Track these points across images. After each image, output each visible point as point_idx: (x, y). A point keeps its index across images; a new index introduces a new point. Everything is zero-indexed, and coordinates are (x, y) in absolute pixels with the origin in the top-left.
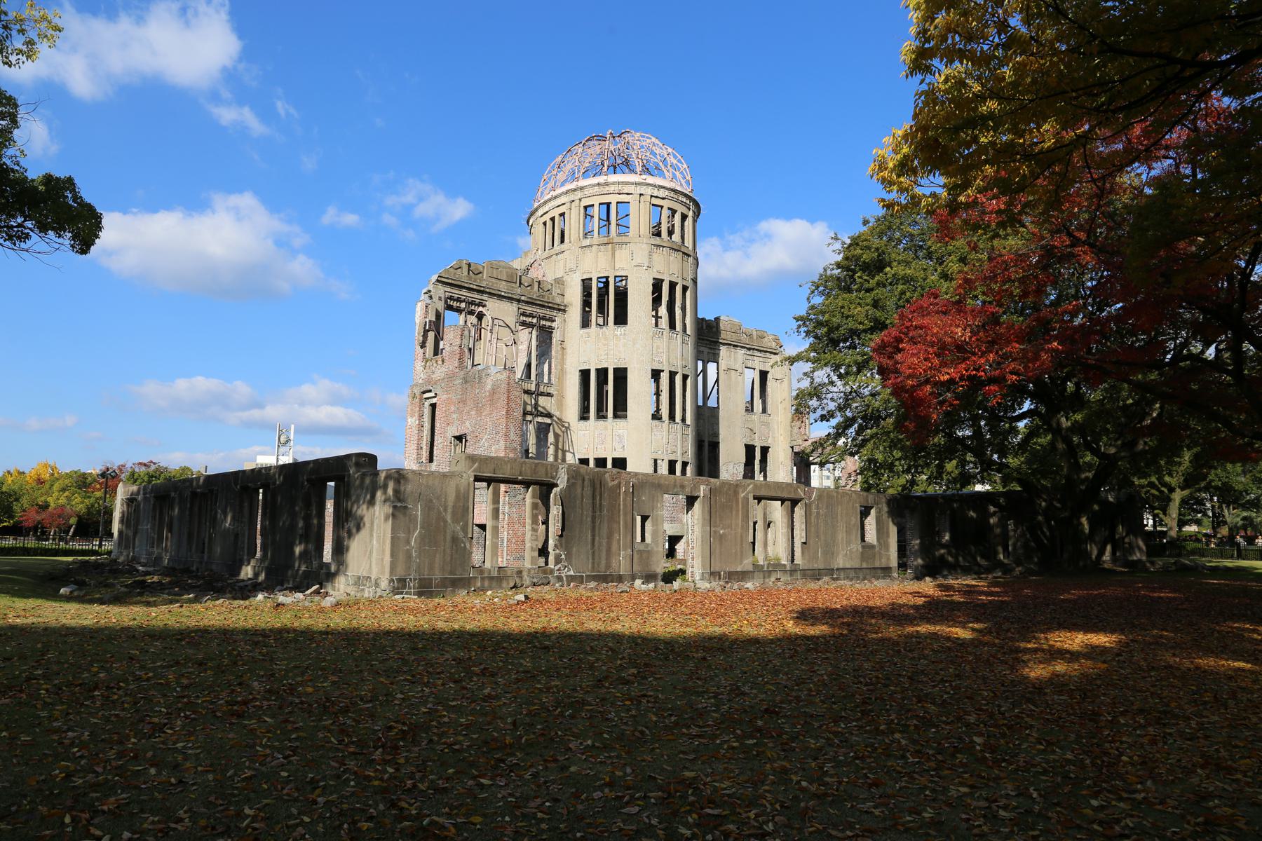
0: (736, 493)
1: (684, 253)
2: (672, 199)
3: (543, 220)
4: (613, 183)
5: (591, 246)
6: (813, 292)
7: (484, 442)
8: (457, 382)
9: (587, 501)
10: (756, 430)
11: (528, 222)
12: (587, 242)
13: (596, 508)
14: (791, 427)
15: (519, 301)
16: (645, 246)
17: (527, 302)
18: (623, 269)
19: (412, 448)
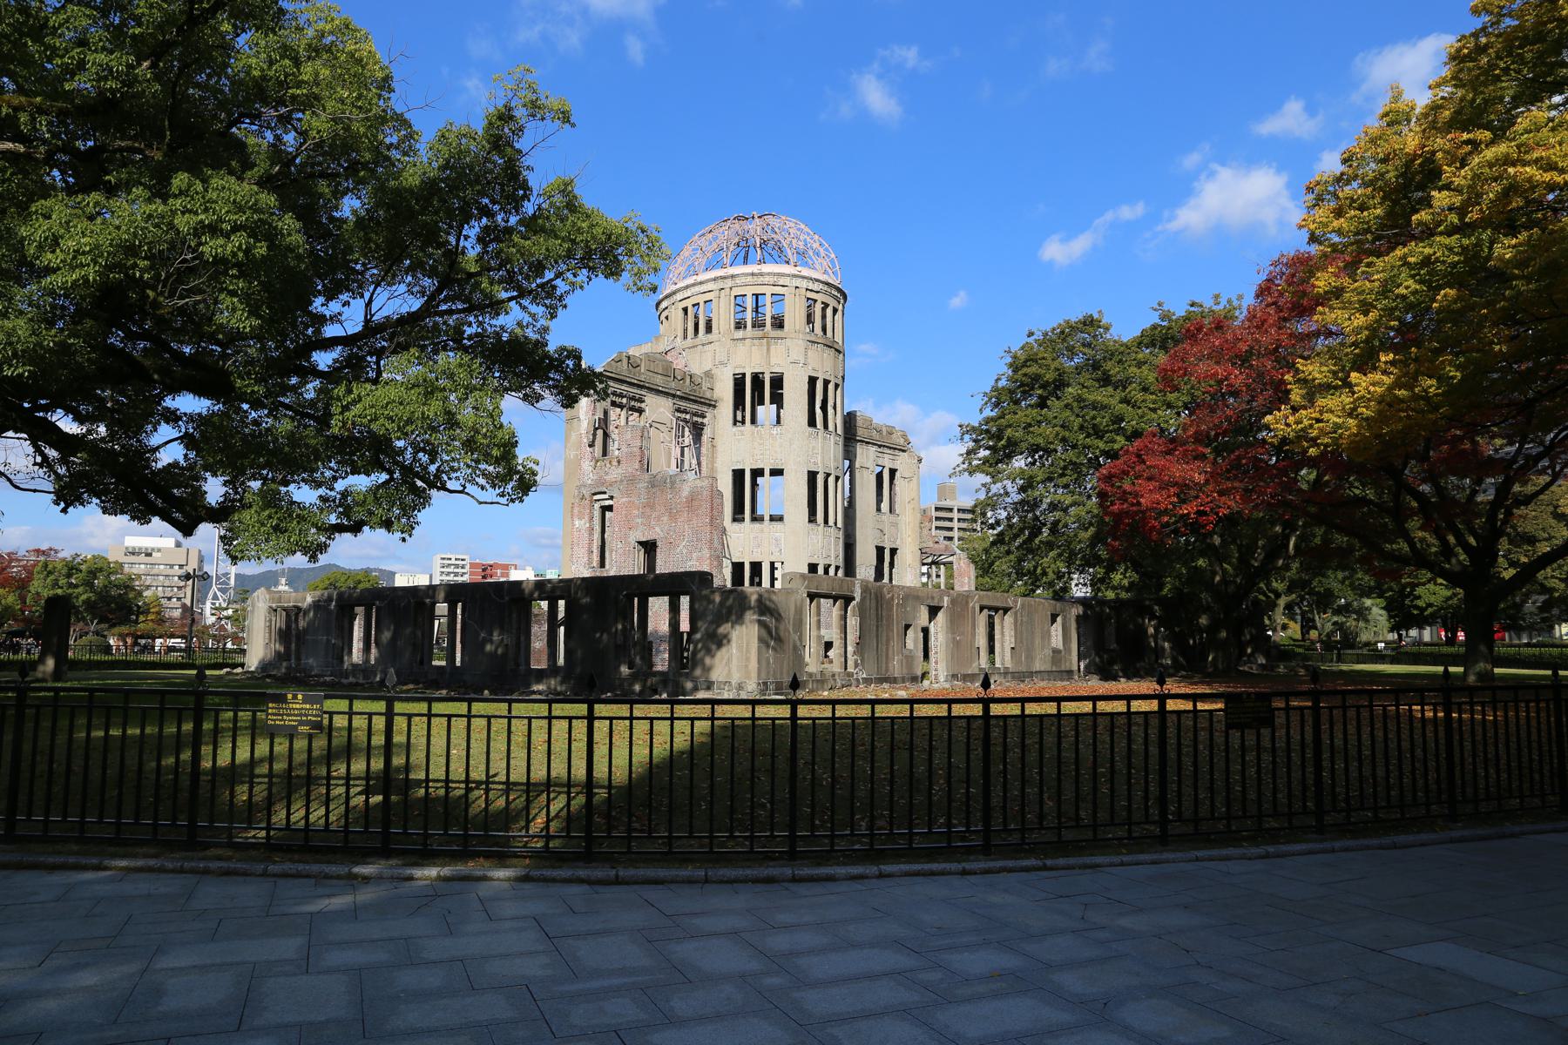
0: (967, 603)
1: (836, 350)
3: (684, 304)
4: (769, 274)
5: (744, 339)
6: (986, 404)
7: (682, 547)
8: (641, 485)
9: (873, 612)
10: (886, 531)
11: (658, 305)
12: (740, 334)
13: (879, 618)
15: (674, 396)
17: (681, 398)
18: (779, 365)
19: (581, 552)
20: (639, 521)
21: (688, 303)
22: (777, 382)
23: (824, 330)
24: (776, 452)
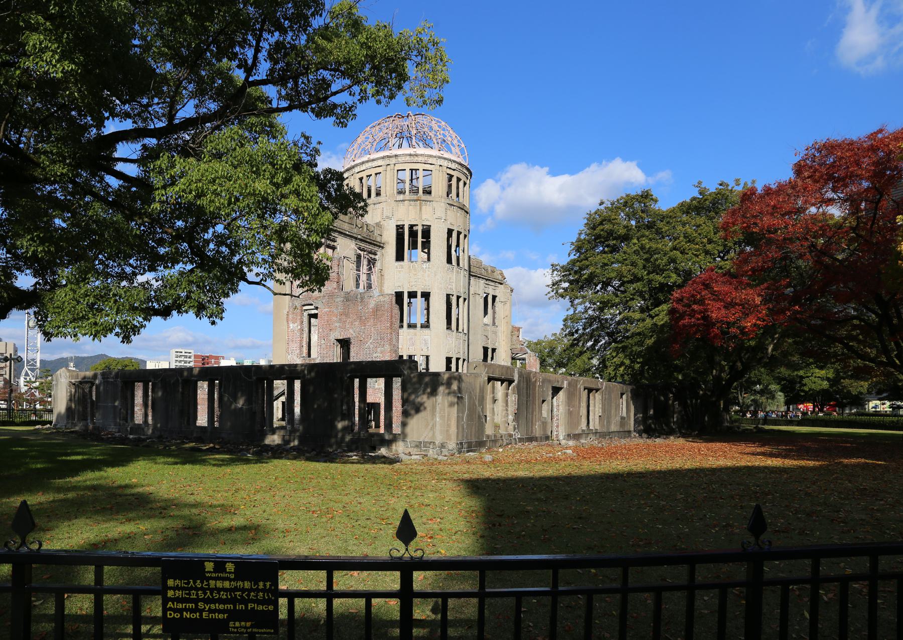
0: (577, 386)
2: (460, 171)
3: (360, 175)
4: (422, 155)
5: (404, 201)
7: (369, 344)
8: (338, 300)
9: (525, 391)
10: (489, 337)
12: (401, 197)
13: (528, 396)
14: (512, 335)
15: (356, 238)
16: (442, 204)
17: (361, 240)
19: (295, 346)
20: (338, 325)
21: (364, 174)
22: (427, 233)
23: (458, 196)
24: (425, 280)
